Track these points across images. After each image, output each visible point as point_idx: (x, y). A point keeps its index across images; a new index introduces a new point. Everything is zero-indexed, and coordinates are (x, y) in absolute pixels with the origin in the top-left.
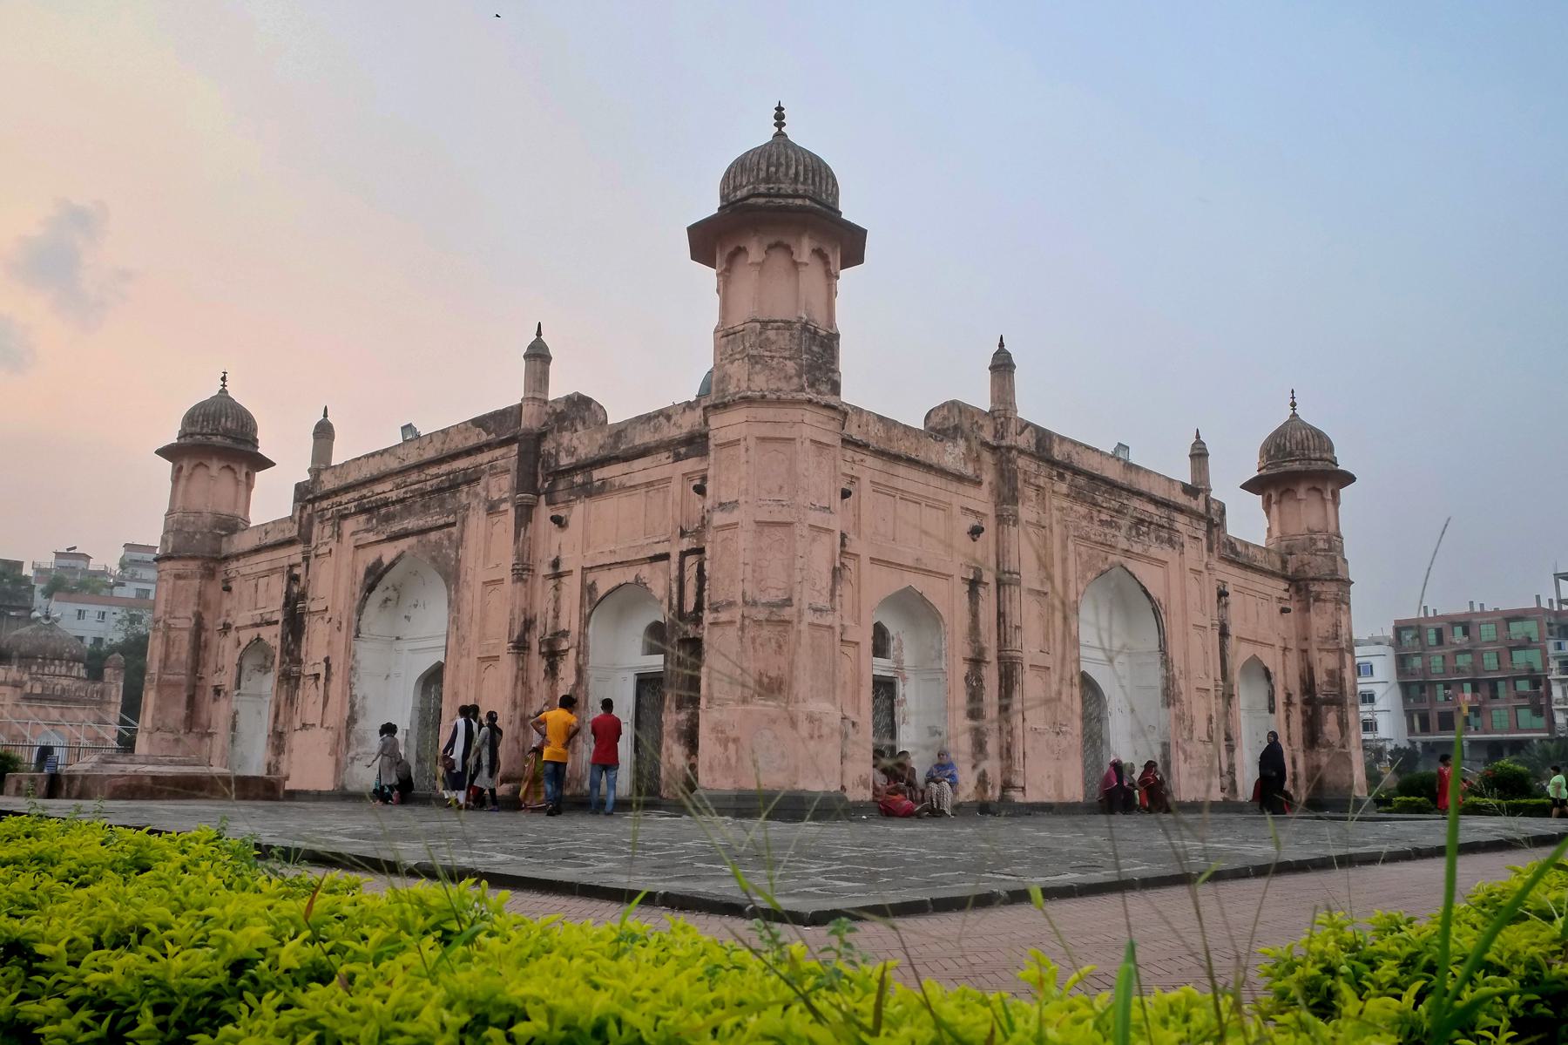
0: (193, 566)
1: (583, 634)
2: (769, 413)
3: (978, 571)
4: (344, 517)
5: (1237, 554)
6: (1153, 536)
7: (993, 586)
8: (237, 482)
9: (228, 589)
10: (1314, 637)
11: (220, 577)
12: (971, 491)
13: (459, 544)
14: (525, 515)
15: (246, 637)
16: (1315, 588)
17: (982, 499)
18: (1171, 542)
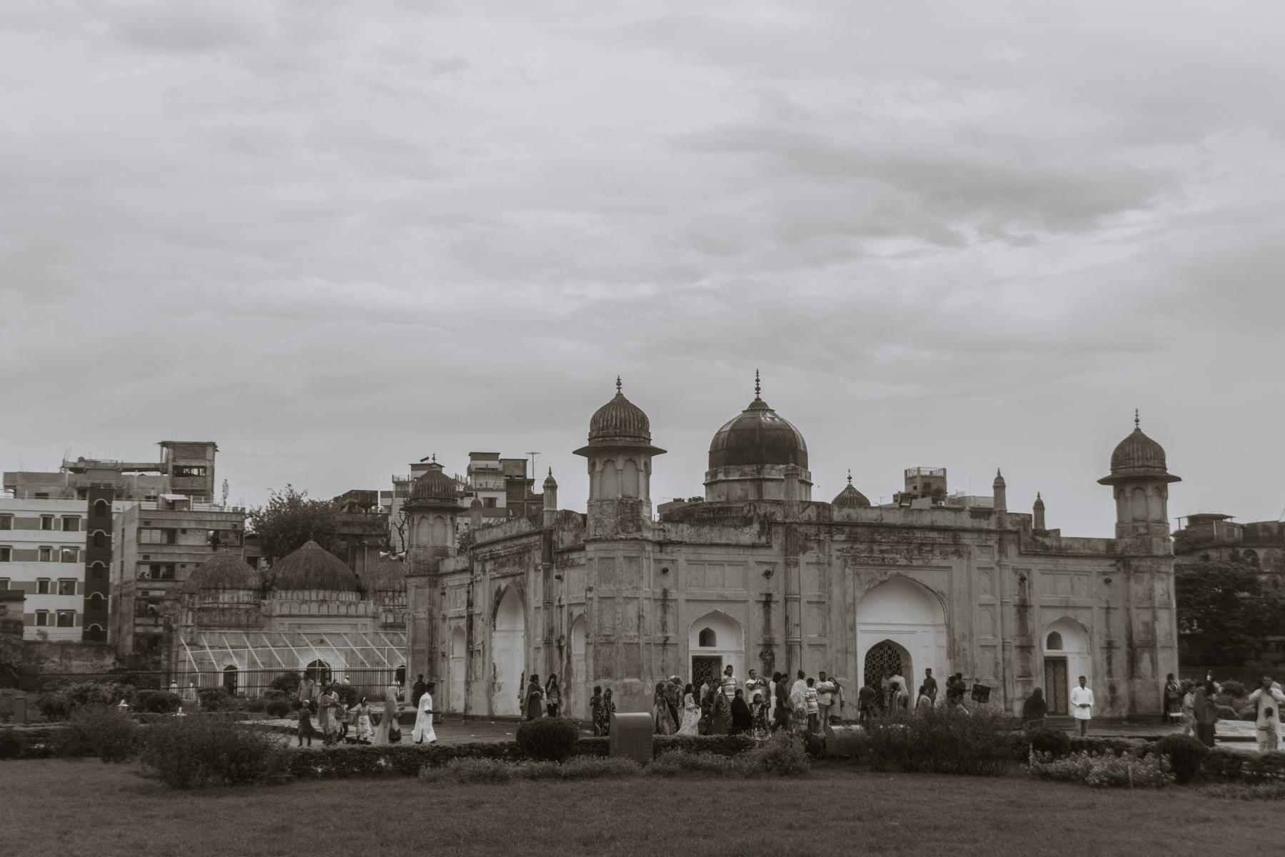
0: (424, 580)
1: (569, 638)
2: (603, 546)
3: (769, 595)
4: (486, 561)
5: (1047, 548)
6: (937, 552)
7: (782, 602)
8: (446, 525)
9: (443, 594)
10: (1132, 599)
11: (440, 586)
12: (763, 552)
13: (526, 585)
14: (547, 572)
15: (453, 623)
16: (1134, 563)
17: (774, 554)
18: (958, 553)
